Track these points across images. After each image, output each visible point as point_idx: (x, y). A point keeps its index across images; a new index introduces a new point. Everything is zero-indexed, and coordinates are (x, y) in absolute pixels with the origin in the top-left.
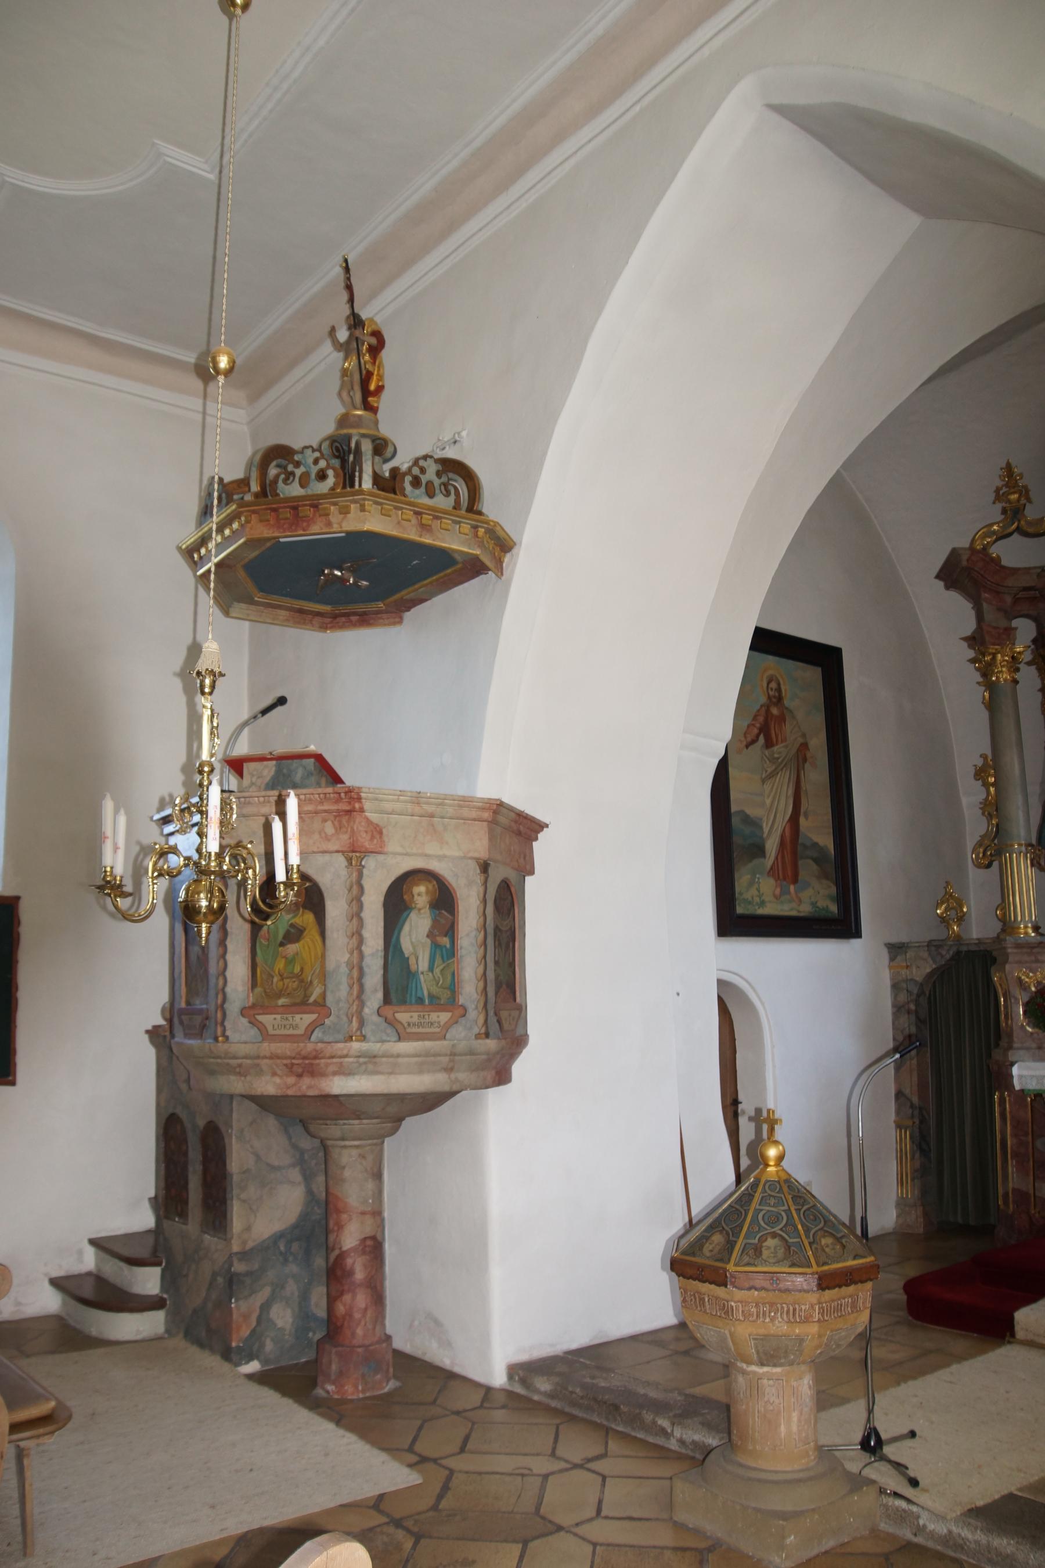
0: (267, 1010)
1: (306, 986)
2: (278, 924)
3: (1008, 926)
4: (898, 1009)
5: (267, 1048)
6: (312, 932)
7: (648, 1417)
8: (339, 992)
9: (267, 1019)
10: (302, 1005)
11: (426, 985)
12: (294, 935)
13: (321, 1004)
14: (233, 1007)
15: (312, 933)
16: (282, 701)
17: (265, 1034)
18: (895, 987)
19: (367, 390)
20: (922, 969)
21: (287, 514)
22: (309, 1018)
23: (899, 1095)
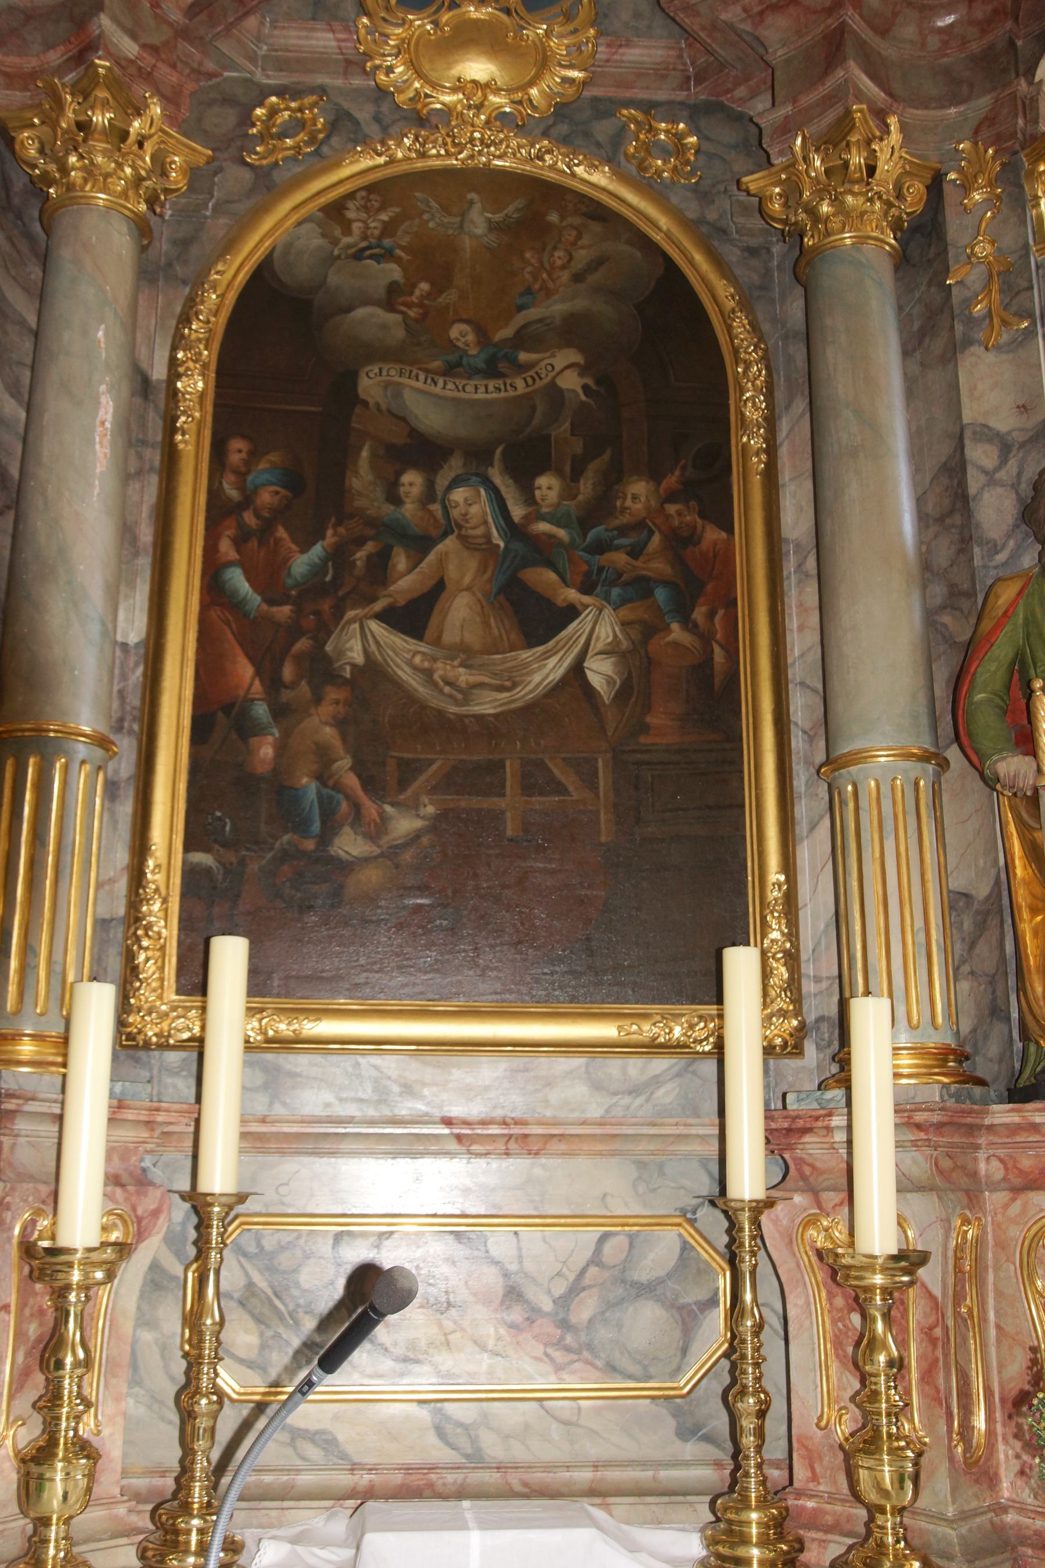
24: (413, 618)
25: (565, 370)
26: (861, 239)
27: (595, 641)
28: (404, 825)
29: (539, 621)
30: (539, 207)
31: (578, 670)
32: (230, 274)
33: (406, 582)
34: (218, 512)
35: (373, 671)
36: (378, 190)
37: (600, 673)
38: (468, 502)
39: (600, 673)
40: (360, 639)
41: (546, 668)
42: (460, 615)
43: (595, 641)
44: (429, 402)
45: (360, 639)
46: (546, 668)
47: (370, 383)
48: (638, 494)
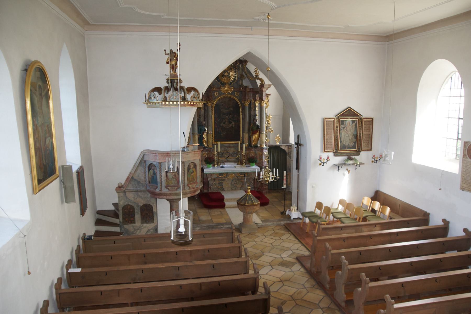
0: (191, 184)
1: (194, 179)
2: (191, 171)
6: (195, 172)
7: (219, 227)
9: (190, 186)
12: (193, 172)
13: (196, 182)
14: (186, 185)
15: (195, 172)
16: (184, 133)
19: (174, 67)
21: (192, 103)
24: (224, 123)
25: (232, 109)
26: (247, 105)
27: (233, 124)
29: (230, 123)
30: (231, 99)
33: (224, 121)
35: (222, 126)
36: (222, 99)
37: (233, 125)
38: (227, 117)
39: (233, 125)
42: (226, 123)
43: (233, 124)
44: (225, 111)
46: (231, 125)
47: (222, 110)
48: (235, 116)
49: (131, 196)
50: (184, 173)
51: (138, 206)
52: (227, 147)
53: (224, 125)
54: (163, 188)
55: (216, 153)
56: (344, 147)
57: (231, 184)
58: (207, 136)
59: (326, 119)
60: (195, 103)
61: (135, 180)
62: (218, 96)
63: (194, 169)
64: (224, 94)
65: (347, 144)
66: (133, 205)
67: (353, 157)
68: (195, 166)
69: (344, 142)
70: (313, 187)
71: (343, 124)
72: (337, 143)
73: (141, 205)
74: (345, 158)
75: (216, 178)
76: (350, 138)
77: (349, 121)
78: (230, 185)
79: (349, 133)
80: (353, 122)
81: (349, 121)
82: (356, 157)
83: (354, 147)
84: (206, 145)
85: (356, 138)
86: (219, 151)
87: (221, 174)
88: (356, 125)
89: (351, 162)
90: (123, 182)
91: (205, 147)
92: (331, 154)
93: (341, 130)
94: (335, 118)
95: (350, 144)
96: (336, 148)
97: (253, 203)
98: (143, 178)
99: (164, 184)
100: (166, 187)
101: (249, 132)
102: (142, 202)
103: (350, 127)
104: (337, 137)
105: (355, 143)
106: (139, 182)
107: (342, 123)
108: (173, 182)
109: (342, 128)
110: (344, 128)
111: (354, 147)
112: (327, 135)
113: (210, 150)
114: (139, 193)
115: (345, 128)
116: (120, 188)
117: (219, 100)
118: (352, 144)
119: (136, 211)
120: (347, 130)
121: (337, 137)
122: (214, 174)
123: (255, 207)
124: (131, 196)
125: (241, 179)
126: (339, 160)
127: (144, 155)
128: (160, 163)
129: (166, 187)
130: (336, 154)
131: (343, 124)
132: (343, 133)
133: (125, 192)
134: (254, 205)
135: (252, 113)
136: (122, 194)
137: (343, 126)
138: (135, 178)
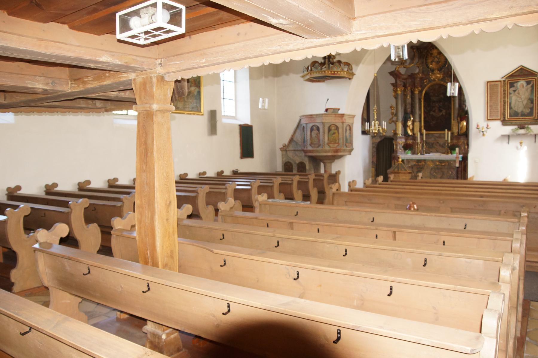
1: (336, 140)
2: (332, 132)
3: (395, 134)
4: (373, 147)
5: (332, 149)
6: (337, 134)
8: (341, 141)
9: (331, 145)
10: (335, 143)
11: (349, 141)
12: (334, 133)
13: (338, 143)
15: (337, 134)
17: (330, 147)
18: (373, 143)
20: (378, 140)
21: (333, 72)
22: (336, 145)
23: (373, 162)
24: (434, 111)
27: (444, 112)
28: (434, 122)
29: (441, 111)
31: (443, 115)
32: (424, 92)
33: (434, 109)
34: (424, 106)
36: (432, 86)
38: (437, 105)
40: (432, 113)
41: (441, 114)
42: (437, 111)
43: (444, 112)
45: (432, 113)
46: (441, 114)
49: (290, 154)
50: (324, 132)
51: (295, 163)
52: (437, 137)
53: (434, 114)
54: (308, 145)
55: (419, 140)
56: (515, 114)
57: (430, 173)
58: (413, 124)
59: (488, 82)
60: (336, 73)
61: (295, 141)
62: (428, 84)
63: (336, 131)
64: (434, 80)
65: (519, 111)
66: (292, 162)
67: (526, 126)
68: (337, 128)
69: (515, 109)
70: (475, 162)
71: (514, 86)
72: (504, 109)
73: (297, 162)
74: (516, 127)
75: (414, 165)
76: (525, 102)
77: (521, 83)
78: (429, 174)
79: (522, 97)
80: (528, 83)
81: (521, 83)
82: (532, 127)
83: (530, 114)
84: (410, 133)
85: (532, 102)
86: (424, 139)
87: (419, 161)
88: (532, 86)
89: (522, 131)
90: (286, 142)
91: (409, 136)
92: (498, 123)
93: (510, 94)
94: (502, 80)
95: (524, 110)
96: (504, 115)
97: (399, 170)
98: (300, 140)
99: (309, 142)
100: (310, 145)
101: (458, 120)
102: (298, 160)
103: (524, 89)
104: (504, 102)
105: (532, 109)
106: (297, 143)
107: (512, 85)
108: (316, 141)
109: (512, 92)
110: (514, 91)
111: (530, 114)
112: (491, 100)
113: (414, 137)
114: (297, 153)
115: (517, 92)
116: (284, 149)
117: (429, 88)
118: (528, 111)
119: (294, 167)
120: (518, 93)
121: (504, 102)
122: (412, 160)
123: (400, 175)
124: (290, 154)
125: (441, 168)
126: (508, 129)
127: (300, 120)
128: (306, 124)
129: (310, 145)
130: (505, 122)
131: (514, 86)
132: (514, 98)
133: (286, 151)
134: (399, 173)
135: (462, 99)
136: (284, 153)
137: (513, 89)
138: (295, 139)
